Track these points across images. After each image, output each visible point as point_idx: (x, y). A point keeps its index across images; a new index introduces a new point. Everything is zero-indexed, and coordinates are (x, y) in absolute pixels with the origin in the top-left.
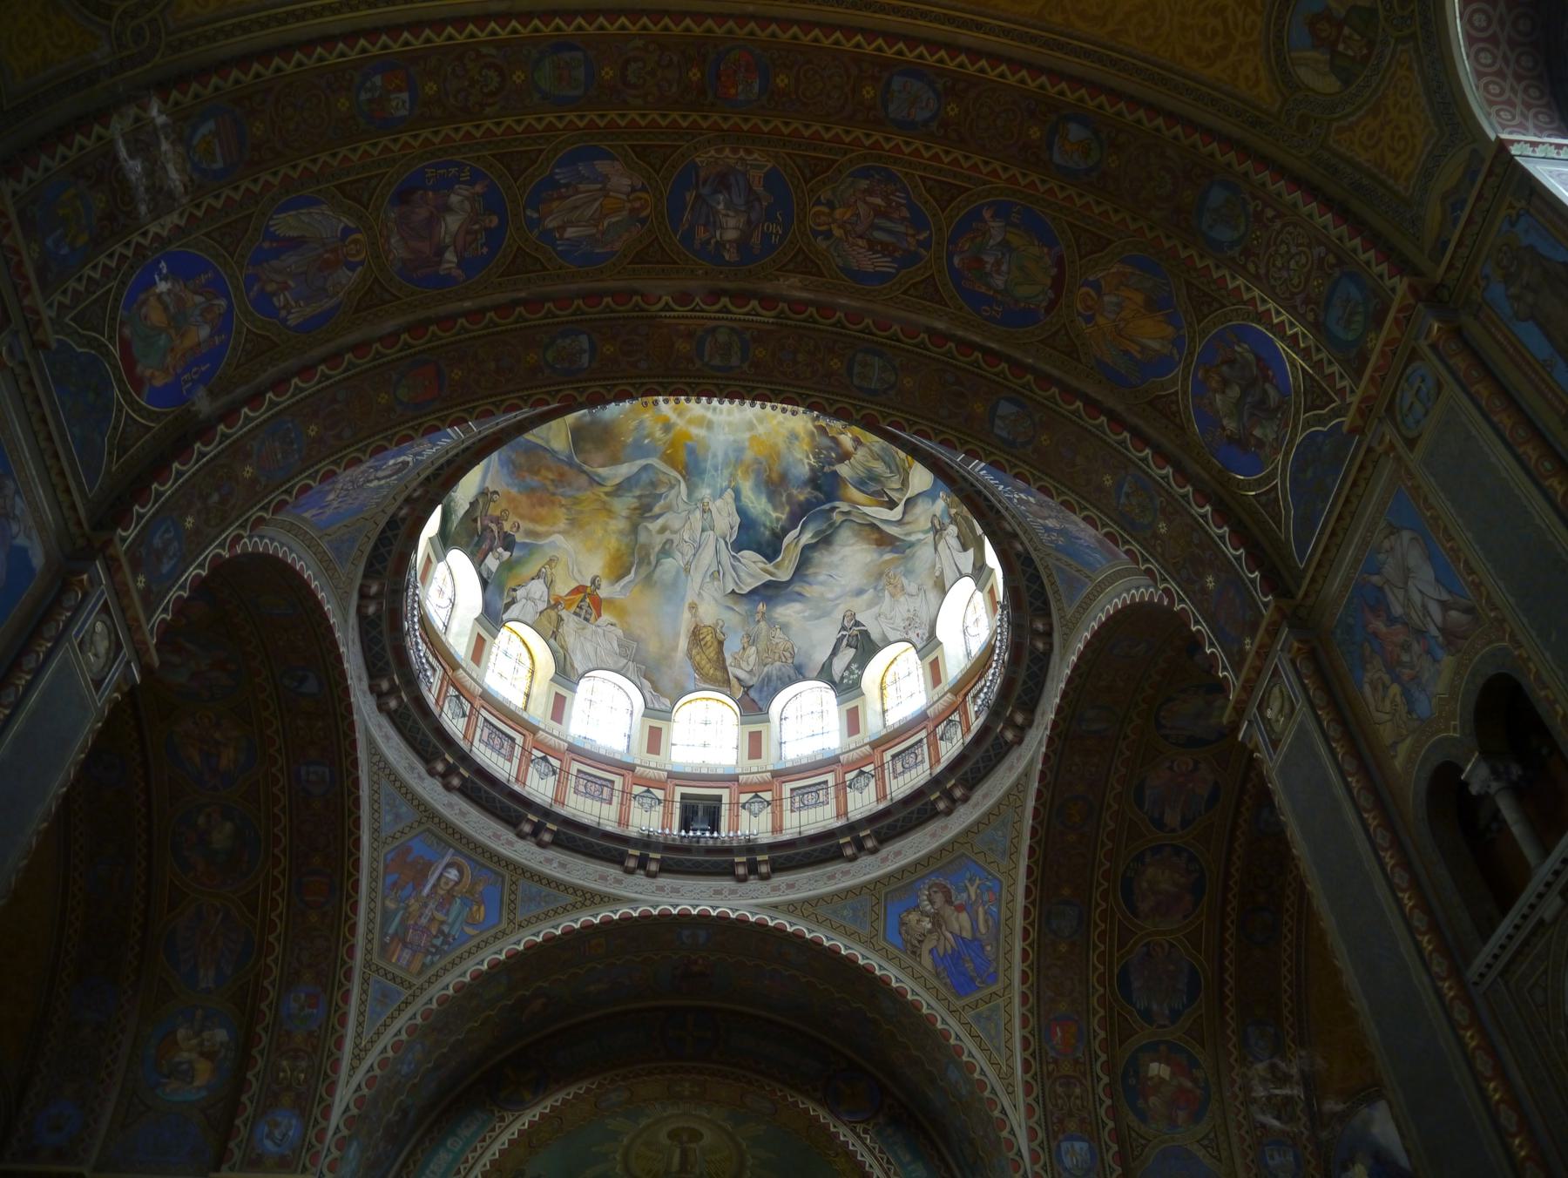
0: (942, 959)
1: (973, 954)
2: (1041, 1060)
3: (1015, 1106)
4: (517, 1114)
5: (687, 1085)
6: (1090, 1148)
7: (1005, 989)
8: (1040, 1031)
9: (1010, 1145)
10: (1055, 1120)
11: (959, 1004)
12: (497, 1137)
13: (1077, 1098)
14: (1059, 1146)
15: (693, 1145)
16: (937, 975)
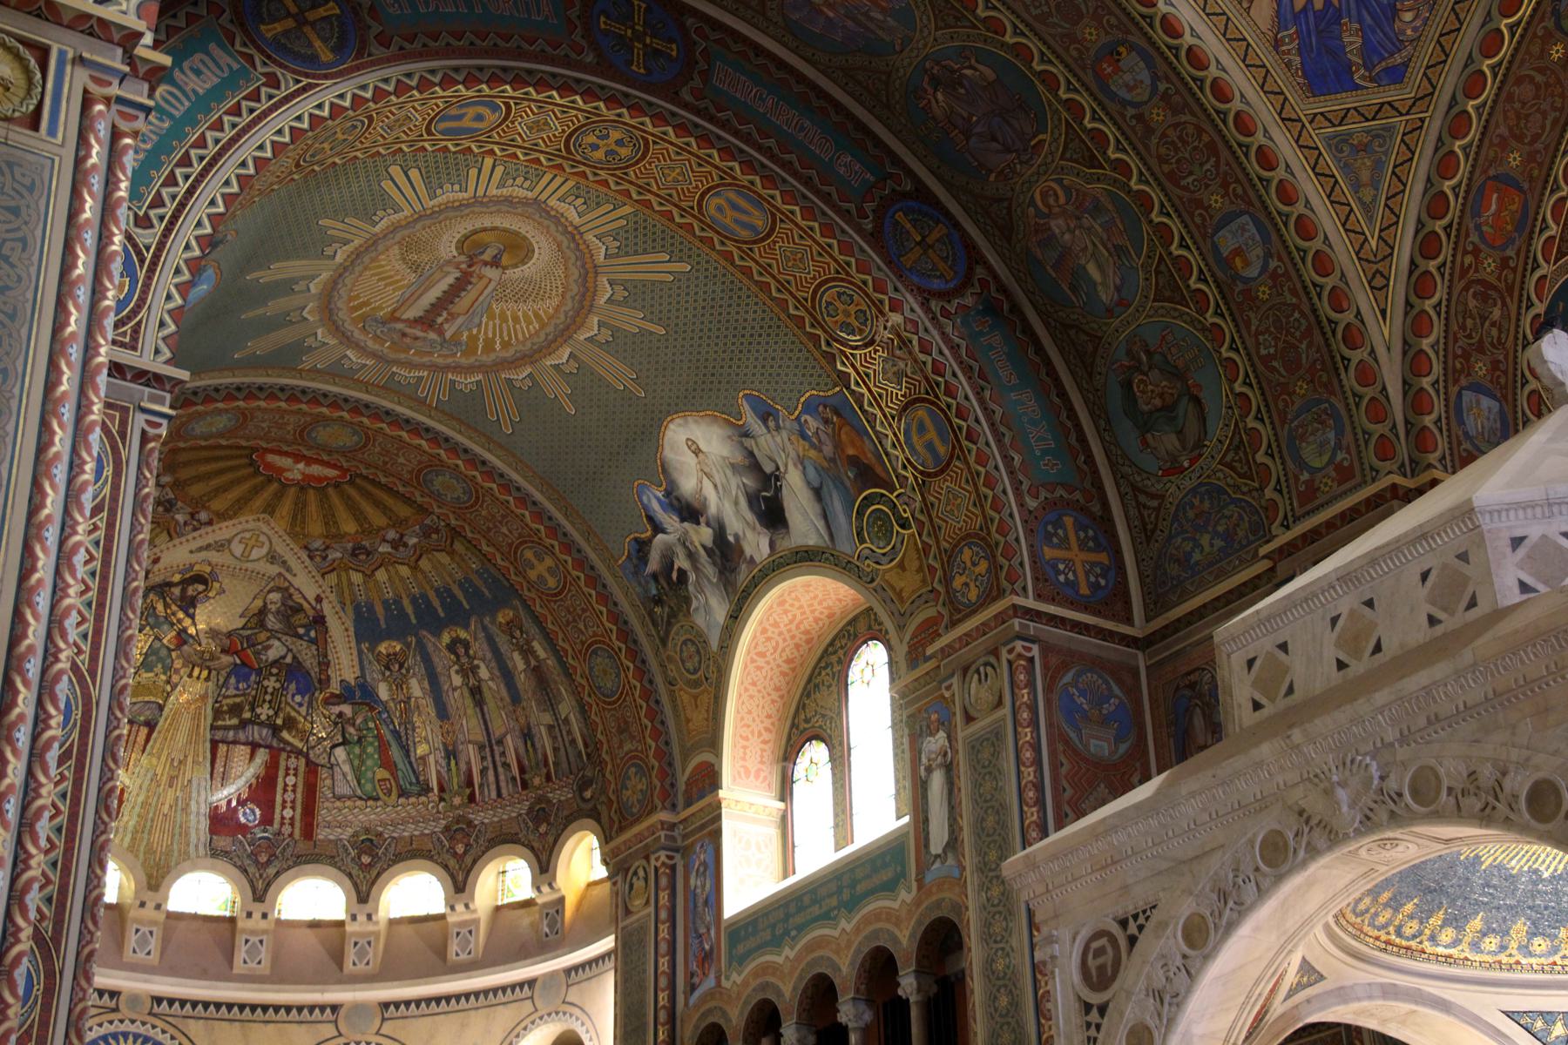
0: (1296, 17)
1: (1368, 19)
2: (1456, 243)
3: (1383, 313)
4: (305, 81)
5: (615, 135)
6: (1502, 412)
7: (1416, 100)
8: (1467, 192)
9: (1367, 375)
10: (1459, 352)
11: (1303, 106)
12: (265, 114)
13: (1493, 324)
14: (1459, 395)
15: (491, 273)
16: (1277, 44)
